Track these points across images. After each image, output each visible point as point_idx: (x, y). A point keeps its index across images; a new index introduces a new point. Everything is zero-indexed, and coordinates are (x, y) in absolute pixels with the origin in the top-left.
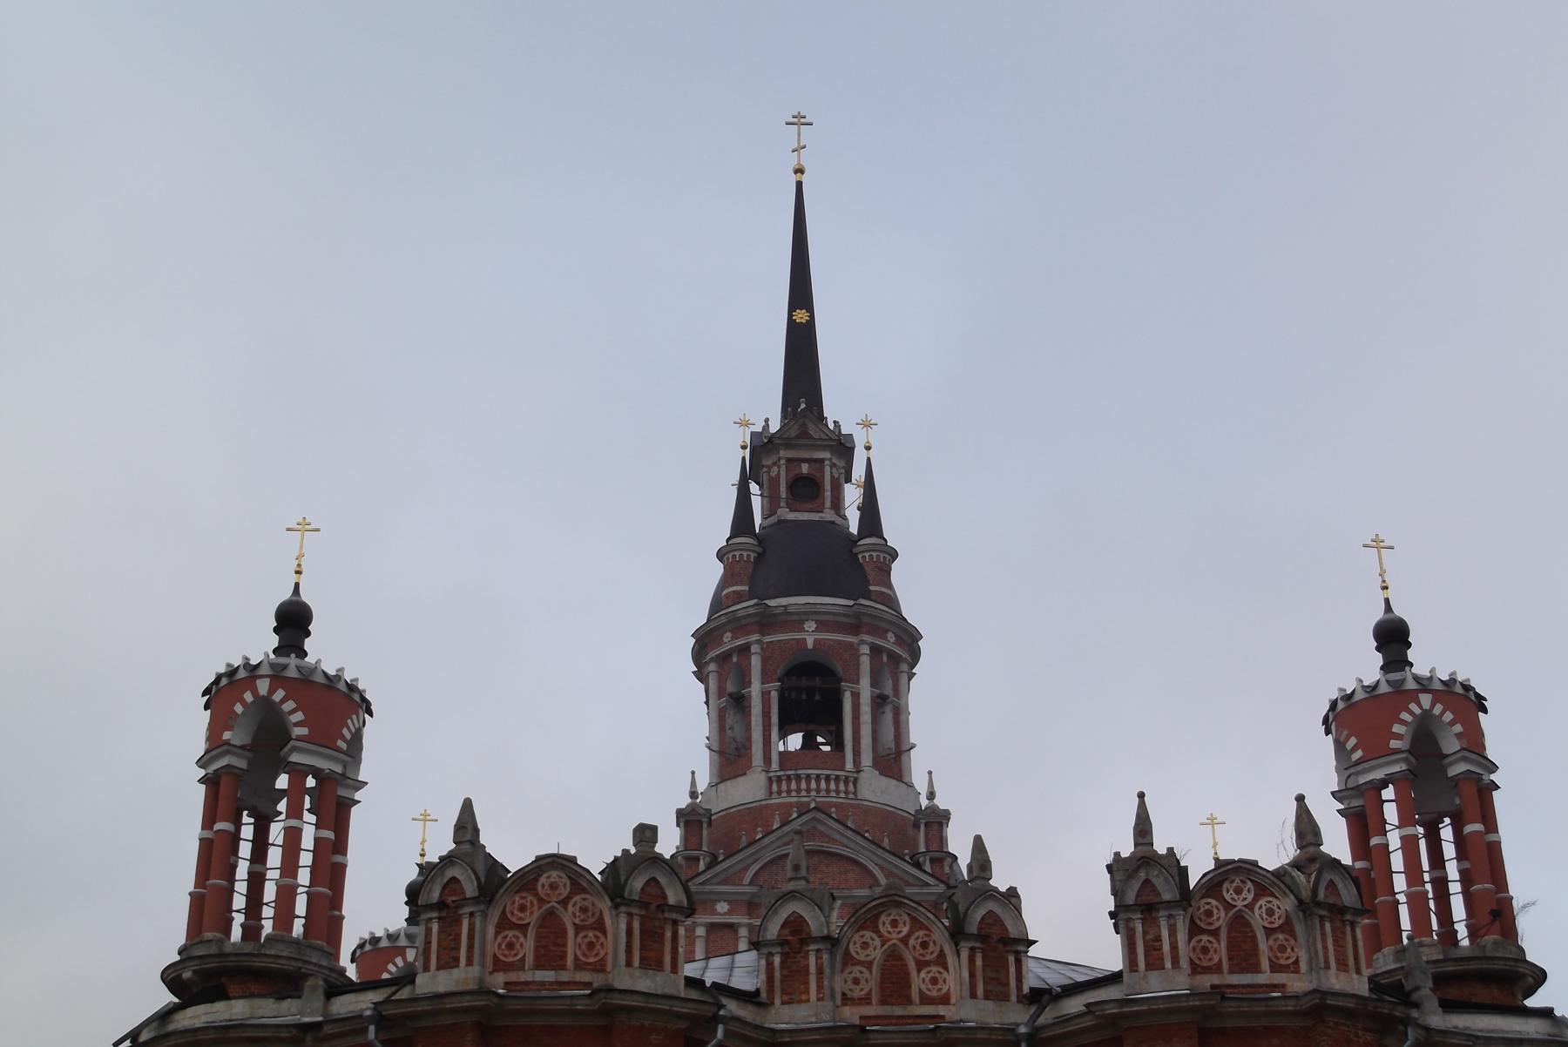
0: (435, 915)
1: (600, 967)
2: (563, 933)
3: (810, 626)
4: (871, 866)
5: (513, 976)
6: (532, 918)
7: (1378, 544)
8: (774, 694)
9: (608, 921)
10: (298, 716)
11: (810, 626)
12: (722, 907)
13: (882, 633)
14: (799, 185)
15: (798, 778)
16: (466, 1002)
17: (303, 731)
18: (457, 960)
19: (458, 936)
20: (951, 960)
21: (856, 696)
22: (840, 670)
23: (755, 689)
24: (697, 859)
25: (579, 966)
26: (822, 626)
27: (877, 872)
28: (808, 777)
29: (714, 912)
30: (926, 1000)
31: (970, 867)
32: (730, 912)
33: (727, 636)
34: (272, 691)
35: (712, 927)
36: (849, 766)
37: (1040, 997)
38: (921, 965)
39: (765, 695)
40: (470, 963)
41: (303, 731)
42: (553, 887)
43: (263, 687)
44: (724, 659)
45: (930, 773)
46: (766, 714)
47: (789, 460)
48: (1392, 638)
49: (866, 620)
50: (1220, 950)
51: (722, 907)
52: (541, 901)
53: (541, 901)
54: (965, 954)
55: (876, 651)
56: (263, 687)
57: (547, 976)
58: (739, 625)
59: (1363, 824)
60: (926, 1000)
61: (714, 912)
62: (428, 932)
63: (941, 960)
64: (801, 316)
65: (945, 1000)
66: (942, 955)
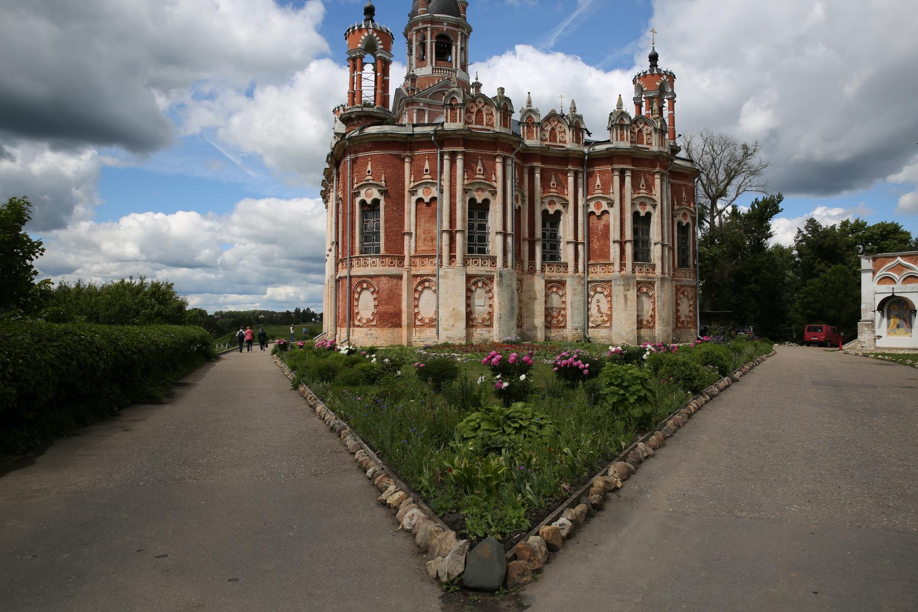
3: (445, 24)
6: (475, 110)
7: (653, 31)
10: (380, 42)
11: (445, 24)
12: (421, 104)
13: (464, 29)
16: (463, 132)
17: (381, 47)
21: (456, 47)
23: (429, 41)
26: (449, 24)
30: (560, 142)
31: (398, 91)
35: (418, 110)
37: (588, 144)
38: (560, 132)
39: (431, 43)
41: (381, 47)
43: (371, 31)
44: (418, 31)
46: (432, 49)
48: (654, 58)
50: (635, 139)
51: (421, 104)
55: (462, 34)
57: (477, 126)
58: (424, 21)
59: (639, 106)
60: (560, 142)
65: (565, 142)
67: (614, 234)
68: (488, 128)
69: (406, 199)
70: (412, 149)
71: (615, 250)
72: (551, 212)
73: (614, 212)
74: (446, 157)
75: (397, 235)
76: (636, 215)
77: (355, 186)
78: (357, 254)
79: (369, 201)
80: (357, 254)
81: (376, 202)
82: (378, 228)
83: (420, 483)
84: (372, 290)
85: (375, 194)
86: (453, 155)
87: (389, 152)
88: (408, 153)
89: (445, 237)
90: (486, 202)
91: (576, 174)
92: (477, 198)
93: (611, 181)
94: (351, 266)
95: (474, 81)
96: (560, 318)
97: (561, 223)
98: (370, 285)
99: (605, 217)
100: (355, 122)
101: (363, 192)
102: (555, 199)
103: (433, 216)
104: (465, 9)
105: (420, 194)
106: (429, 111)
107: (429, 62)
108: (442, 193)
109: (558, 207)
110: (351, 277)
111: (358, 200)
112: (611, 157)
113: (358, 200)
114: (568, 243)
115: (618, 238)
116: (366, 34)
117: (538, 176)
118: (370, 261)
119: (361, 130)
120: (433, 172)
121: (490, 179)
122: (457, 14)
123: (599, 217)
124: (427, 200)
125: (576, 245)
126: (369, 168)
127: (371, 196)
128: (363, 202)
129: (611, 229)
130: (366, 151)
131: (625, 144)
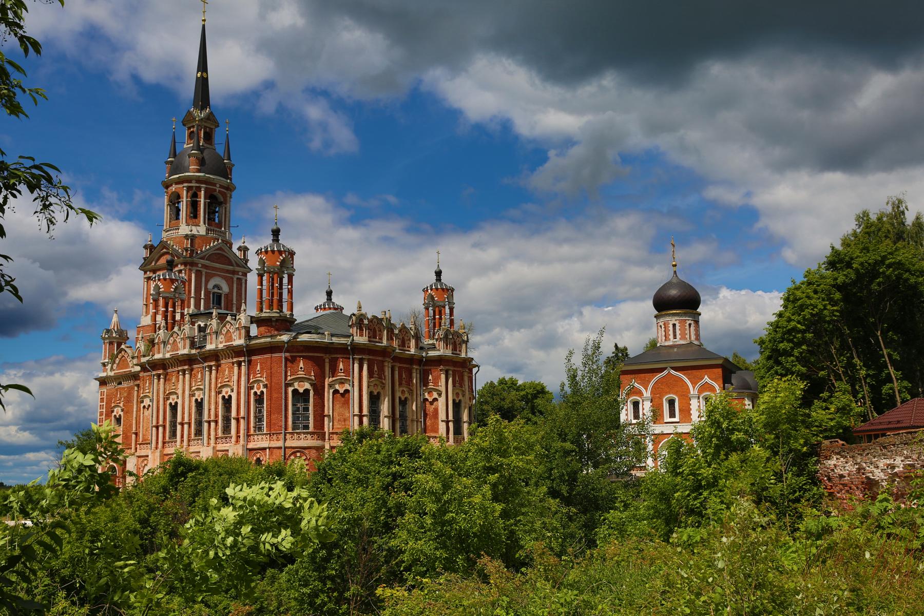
14: (204, 26)
39: (205, 203)
48: (438, 274)
58: (199, 180)
63: (409, 340)
64: (205, 75)
67: (442, 416)
70: (330, 353)
71: (442, 427)
72: (403, 399)
73: (442, 401)
75: (320, 417)
76: (454, 400)
77: (289, 378)
78: (290, 430)
79: (301, 390)
80: (290, 430)
81: (307, 391)
82: (307, 409)
83: (479, 556)
84: (304, 458)
85: (307, 386)
87: (316, 355)
89: (356, 419)
90: (379, 393)
93: (439, 377)
94: (285, 440)
98: (303, 454)
99: (435, 403)
101: (296, 384)
103: (346, 403)
104: (231, 171)
107: (202, 222)
108: (353, 386)
109: (407, 395)
110: (285, 448)
111: (290, 389)
112: (439, 361)
113: (290, 389)
114: (412, 421)
115: (444, 418)
117: (397, 373)
118: (302, 436)
119: (295, 338)
120: (346, 372)
121: (380, 378)
122: (228, 178)
123: (431, 403)
124: (342, 391)
126: (301, 365)
128: (295, 392)
129: (440, 411)
130: (298, 352)
131: (449, 352)
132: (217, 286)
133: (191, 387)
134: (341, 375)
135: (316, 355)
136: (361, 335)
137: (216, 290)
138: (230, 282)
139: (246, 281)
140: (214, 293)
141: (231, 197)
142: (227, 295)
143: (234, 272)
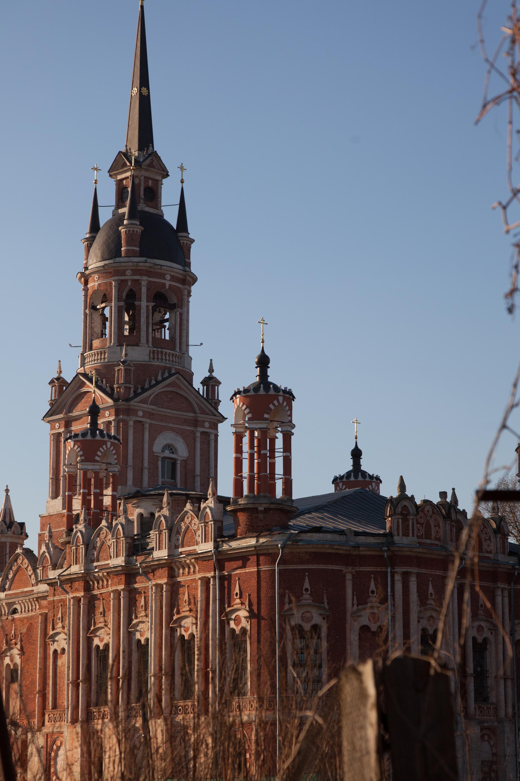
0: (400, 517)
1: (439, 539)
2: (430, 527)
3: (168, 277)
4: (194, 403)
5: (420, 540)
8: (151, 307)
9: (441, 525)
11: (168, 277)
12: (140, 413)
15: (162, 352)
18: (409, 533)
19: (408, 526)
20: (492, 539)
22: (174, 300)
24: (130, 388)
25: (436, 539)
27: (195, 406)
28: (166, 352)
29: (137, 415)
30: (487, 552)
32: (143, 417)
33: (129, 272)
34: (283, 402)
35: (136, 422)
36: (178, 349)
38: (486, 540)
39: (147, 307)
40: (413, 536)
42: (428, 511)
43: (281, 399)
45: (211, 360)
47: (145, 177)
49: (188, 278)
51: (140, 413)
52: (425, 515)
53: (425, 515)
54: (498, 539)
56: (281, 399)
61: (137, 415)
62: (398, 522)
63: (490, 539)
64: (144, 89)
65: (490, 552)
66: (490, 537)
68: (437, 542)
69: (348, 625)
72: (480, 640)
74: (398, 577)
85: (317, 619)
86: (406, 576)
87: (330, 567)
88: (350, 569)
91: (503, 590)
92: (428, 627)
95: (207, 374)
96: (493, 775)
97: (488, 653)
100: (261, 516)
102: (483, 624)
105: (364, 621)
106: (150, 425)
109: (487, 634)
116: (276, 402)
125: (505, 680)
126: (307, 585)
127: (309, 620)
130: (301, 563)
132: (170, 447)
133: (129, 620)
134: (374, 599)
135: (330, 567)
136: (406, 534)
137: (167, 453)
138: (189, 440)
139: (216, 436)
140: (164, 458)
141: (189, 295)
142: (185, 462)
143: (196, 423)
